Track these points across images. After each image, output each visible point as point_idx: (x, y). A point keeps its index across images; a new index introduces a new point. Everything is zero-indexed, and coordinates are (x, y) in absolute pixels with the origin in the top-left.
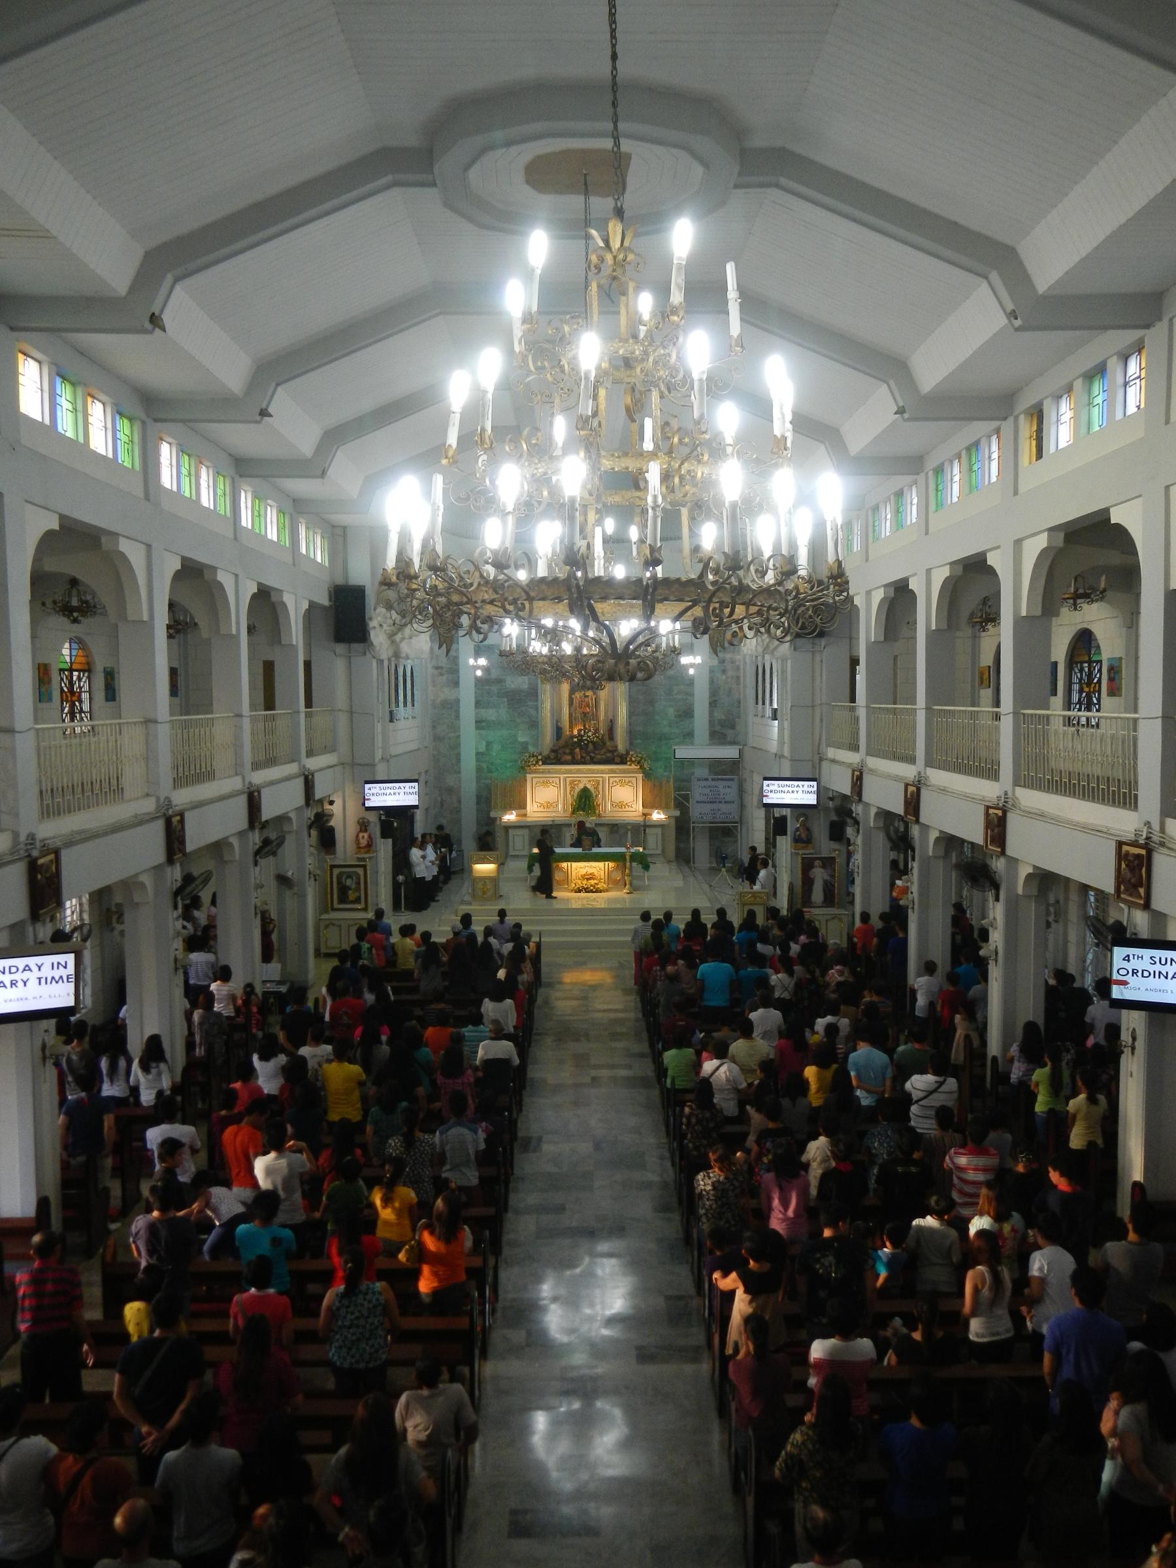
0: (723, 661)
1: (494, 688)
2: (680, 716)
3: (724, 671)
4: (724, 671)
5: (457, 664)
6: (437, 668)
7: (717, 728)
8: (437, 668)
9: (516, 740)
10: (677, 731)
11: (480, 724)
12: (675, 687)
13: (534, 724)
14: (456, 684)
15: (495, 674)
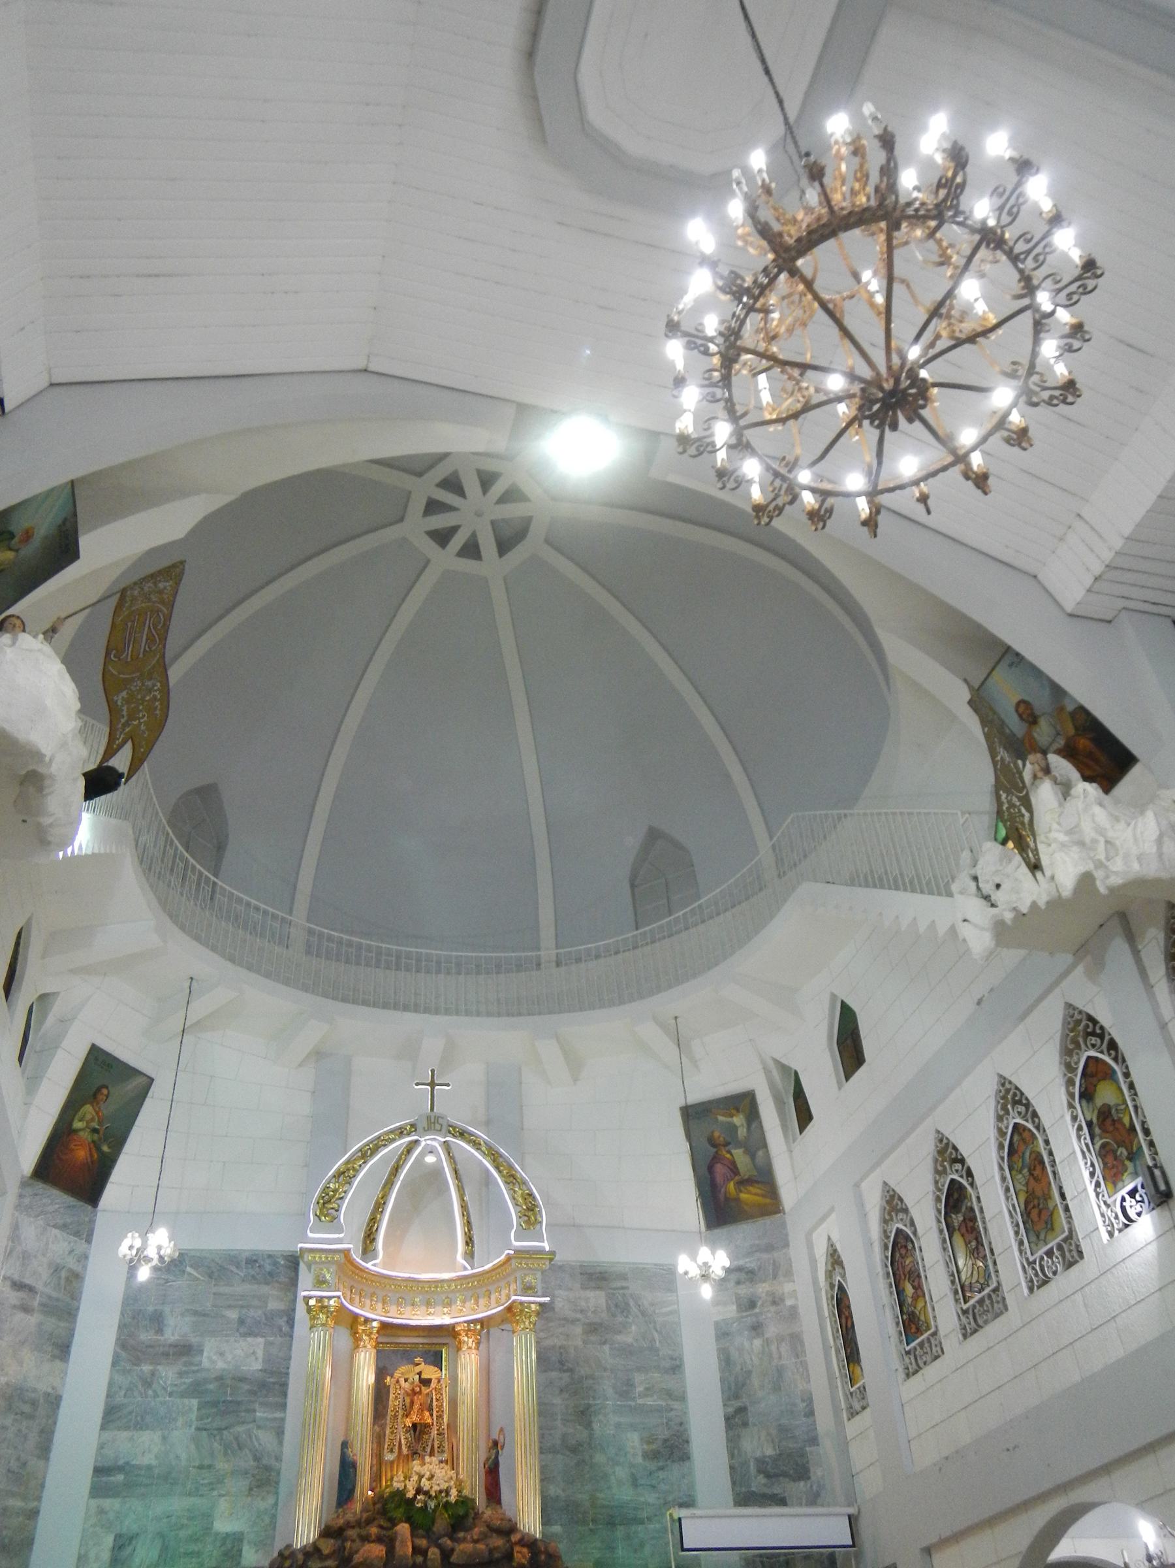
0: (752, 1304)
1: (168, 1373)
2: (653, 1456)
3: (757, 1328)
4: (757, 1328)
5: (75, 1296)
6: (18, 1286)
7: (758, 1483)
8: (18, 1286)
9: (208, 1529)
10: (651, 1498)
11: (108, 1477)
12: (638, 1378)
13: (265, 1478)
14: (62, 1349)
15: (176, 1329)
